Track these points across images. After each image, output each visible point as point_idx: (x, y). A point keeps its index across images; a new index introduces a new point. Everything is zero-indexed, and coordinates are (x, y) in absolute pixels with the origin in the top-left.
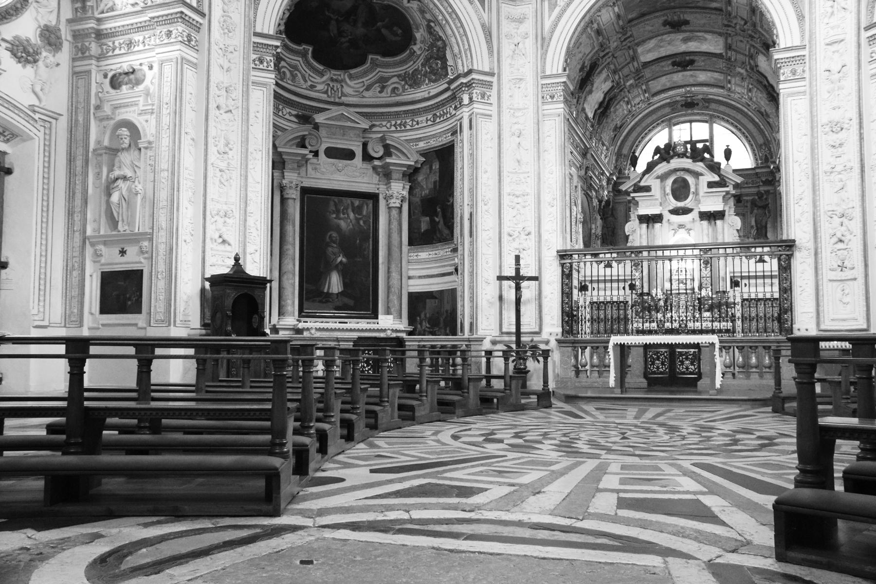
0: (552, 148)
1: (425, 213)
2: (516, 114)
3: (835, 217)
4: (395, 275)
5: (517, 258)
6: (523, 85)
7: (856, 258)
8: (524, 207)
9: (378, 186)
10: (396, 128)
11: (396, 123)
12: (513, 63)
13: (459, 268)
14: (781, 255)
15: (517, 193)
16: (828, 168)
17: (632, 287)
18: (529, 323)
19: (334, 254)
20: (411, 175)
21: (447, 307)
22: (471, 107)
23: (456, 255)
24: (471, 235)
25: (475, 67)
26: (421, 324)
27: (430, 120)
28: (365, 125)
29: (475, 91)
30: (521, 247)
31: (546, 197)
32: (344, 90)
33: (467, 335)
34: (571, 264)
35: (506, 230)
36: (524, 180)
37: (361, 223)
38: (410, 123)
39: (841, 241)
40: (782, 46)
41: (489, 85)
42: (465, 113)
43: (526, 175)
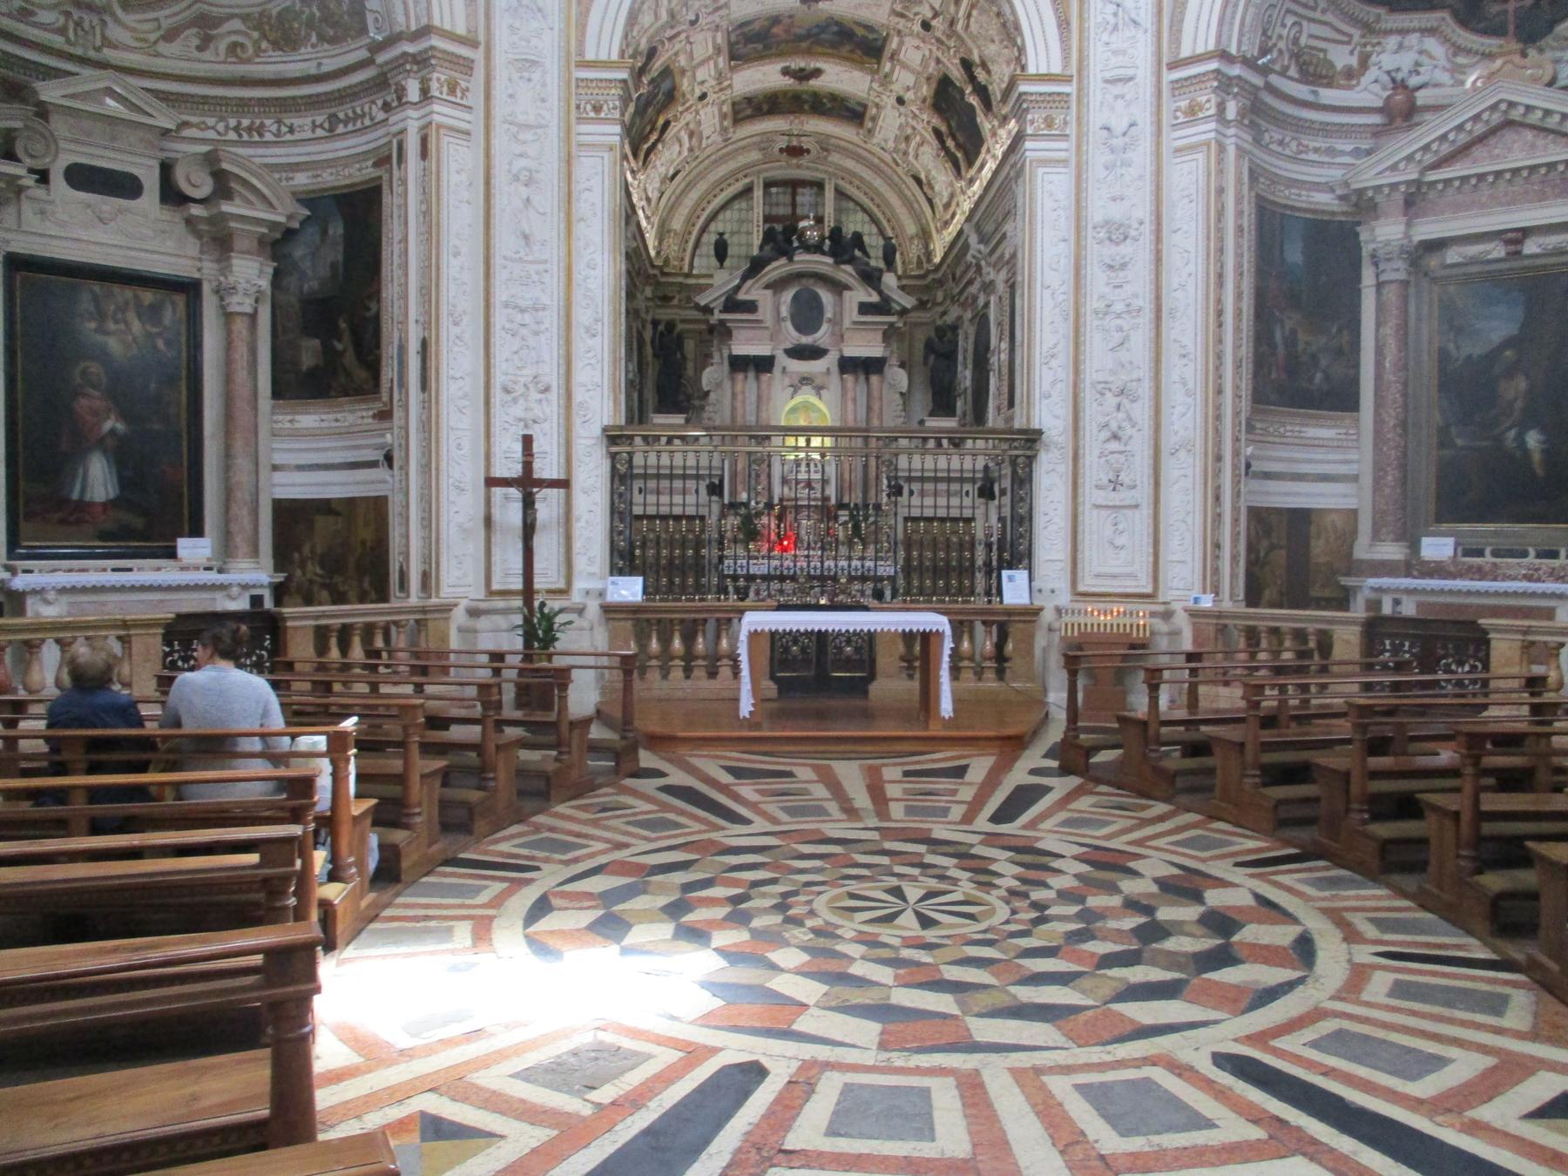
0: (595, 215)
1: (308, 330)
2: (522, 136)
3: (1109, 395)
4: (242, 463)
5: (527, 441)
6: (536, 77)
7: (1139, 469)
8: (536, 333)
9: (199, 264)
10: (240, 136)
11: (239, 123)
12: (517, 25)
13: (396, 455)
14: (1017, 456)
15: (523, 303)
16: (1100, 305)
17: (715, 489)
18: (547, 574)
19: (95, 413)
20: (278, 244)
21: (366, 534)
22: (427, 110)
23: (386, 425)
24: (424, 385)
25: (436, 22)
26: (303, 566)
27: (321, 126)
28: (165, 119)
29: (435, 75)
30: (530, 415)
31: (582, 316)
32: (108, 33)
33: (414, 599)
34: (631, 455)
35: (498, 379)
36: (536, 278)
37: (160, 344)
38: (274, 128)
39: (1115, 437)
40: (1032, 70)
41: (467, 66)
42: (411, 119)
43: (541, 267)
